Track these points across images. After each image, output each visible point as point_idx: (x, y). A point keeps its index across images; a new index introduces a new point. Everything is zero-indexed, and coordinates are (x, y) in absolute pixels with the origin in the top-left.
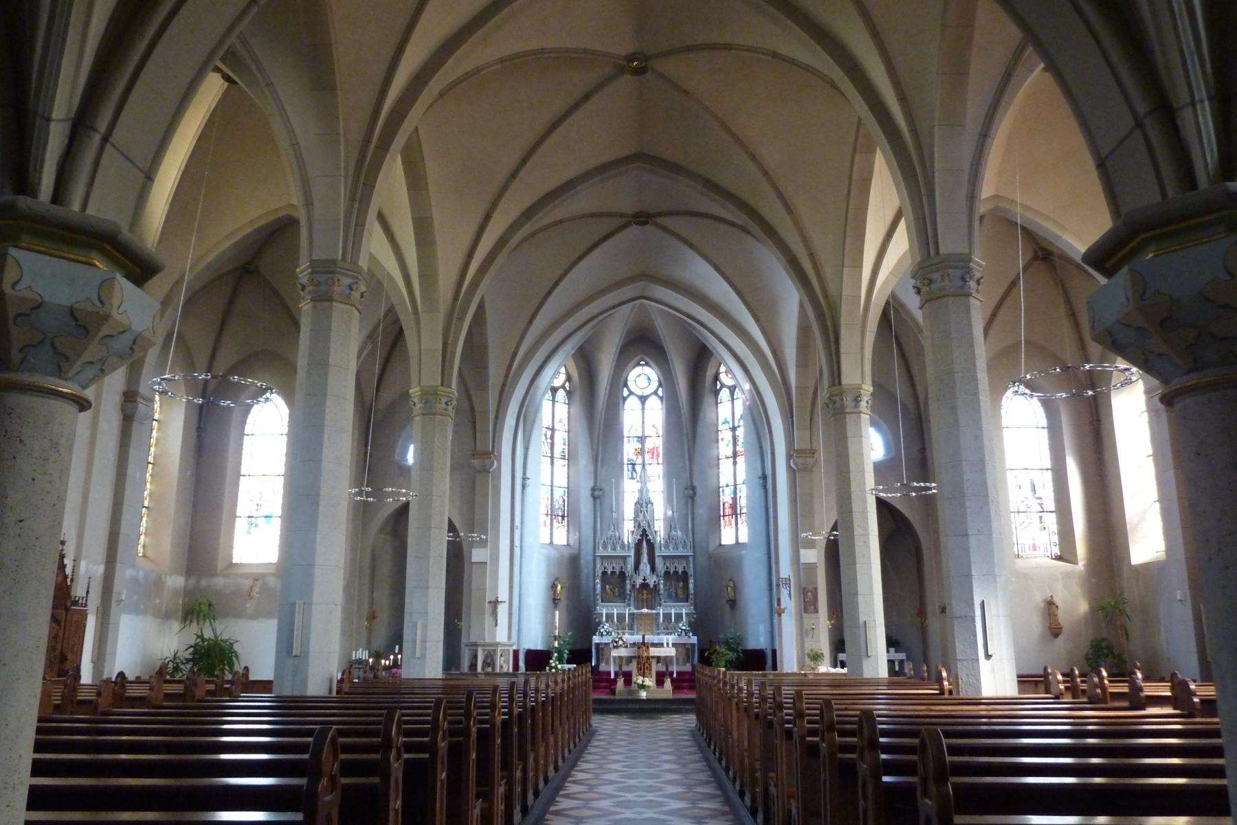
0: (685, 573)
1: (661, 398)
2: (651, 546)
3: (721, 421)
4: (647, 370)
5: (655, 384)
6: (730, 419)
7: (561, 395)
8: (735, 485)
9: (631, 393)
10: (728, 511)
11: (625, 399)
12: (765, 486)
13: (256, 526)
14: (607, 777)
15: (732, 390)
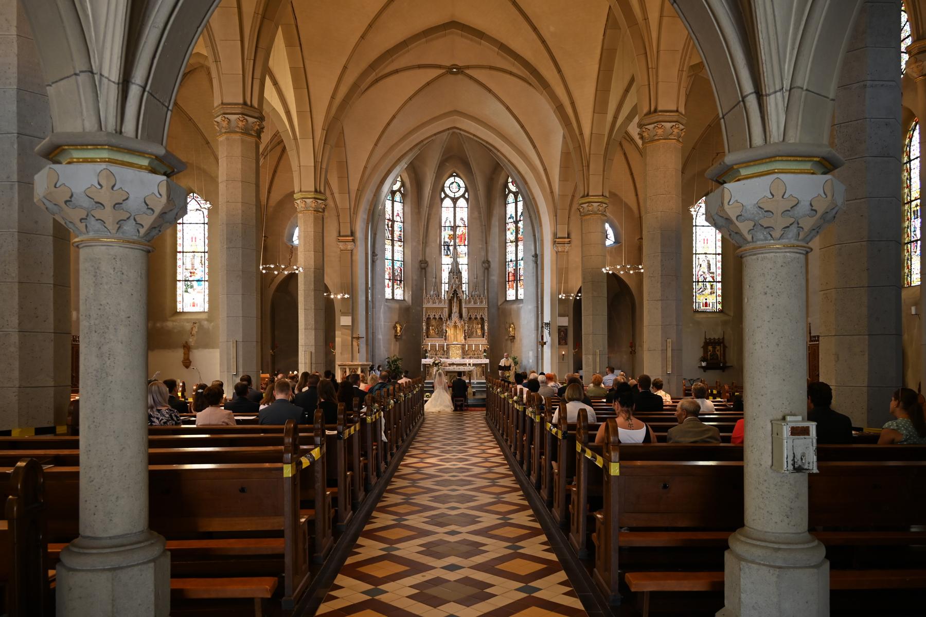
0: (482, 319)
1: (467, 200)
2: (460, 301)
3: (508, 216)
4: (457, 179)
5: (462, 190)
6: (514, 215)
7: (398, 197)
8: (517, 260)
9: (447, 196)
10: (511, 278)
11: (442, 200)
12: (536, 262)
13: (192, 287)
14: (431, 452)
15: (516, 195)
